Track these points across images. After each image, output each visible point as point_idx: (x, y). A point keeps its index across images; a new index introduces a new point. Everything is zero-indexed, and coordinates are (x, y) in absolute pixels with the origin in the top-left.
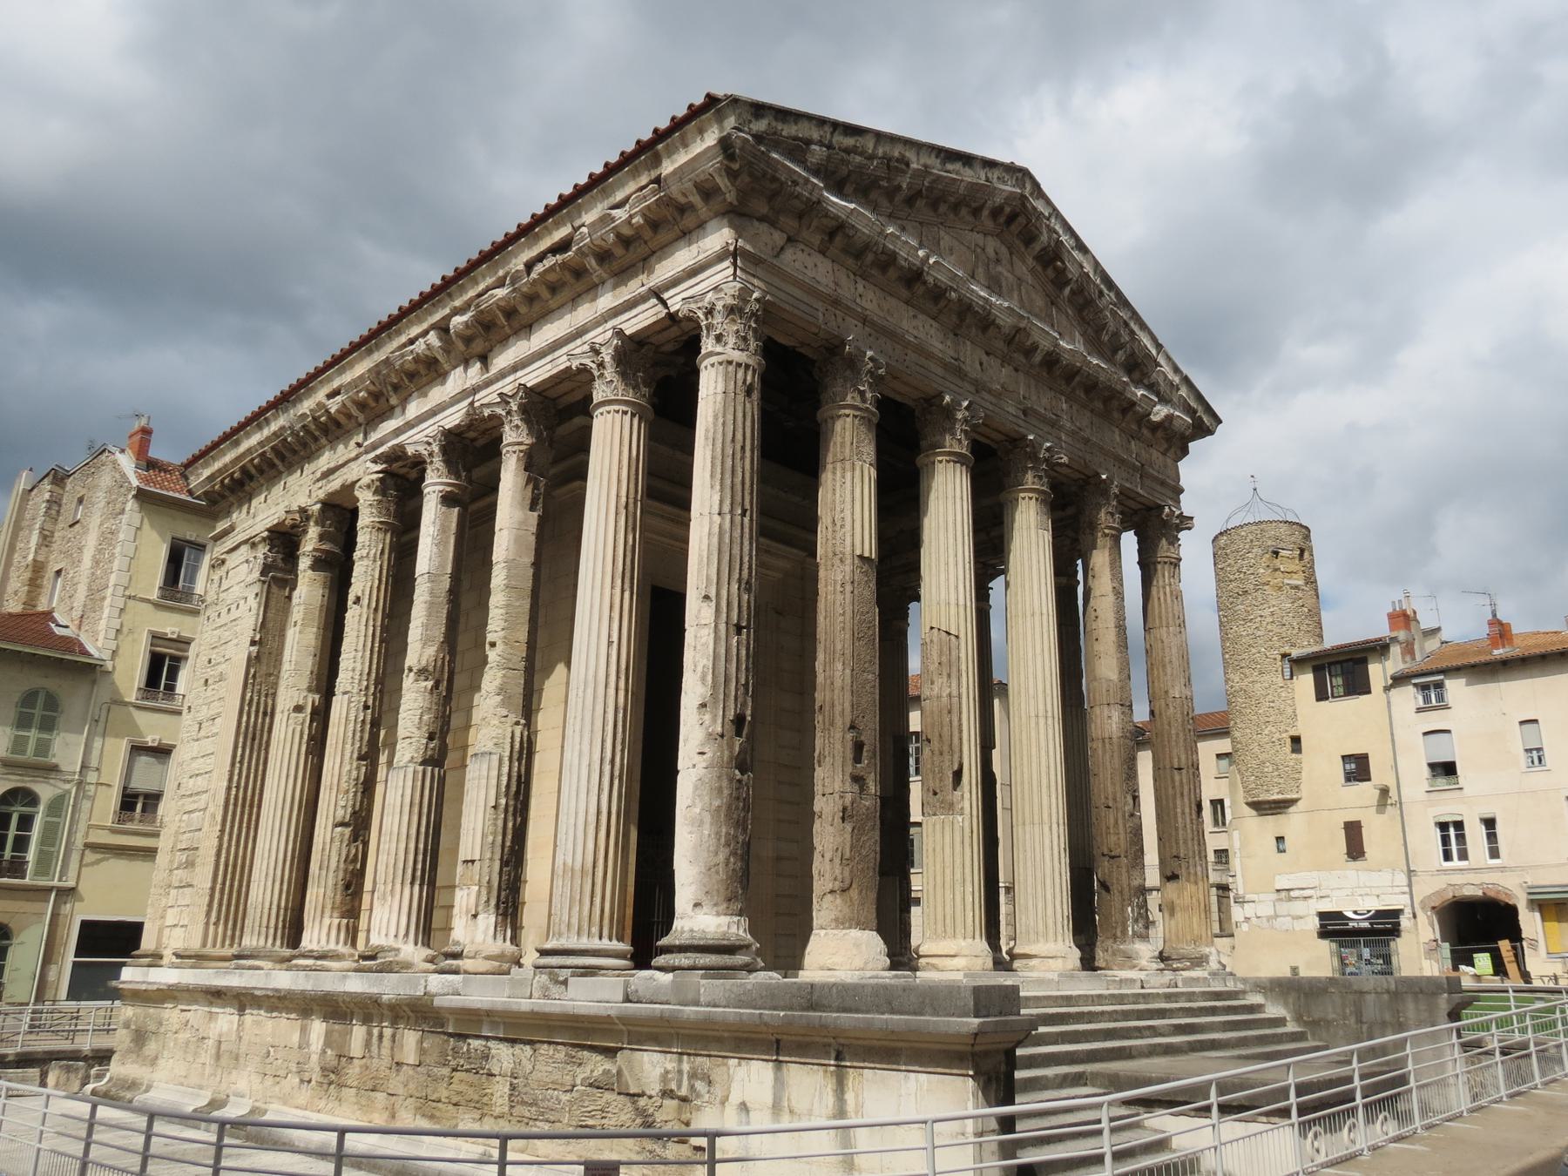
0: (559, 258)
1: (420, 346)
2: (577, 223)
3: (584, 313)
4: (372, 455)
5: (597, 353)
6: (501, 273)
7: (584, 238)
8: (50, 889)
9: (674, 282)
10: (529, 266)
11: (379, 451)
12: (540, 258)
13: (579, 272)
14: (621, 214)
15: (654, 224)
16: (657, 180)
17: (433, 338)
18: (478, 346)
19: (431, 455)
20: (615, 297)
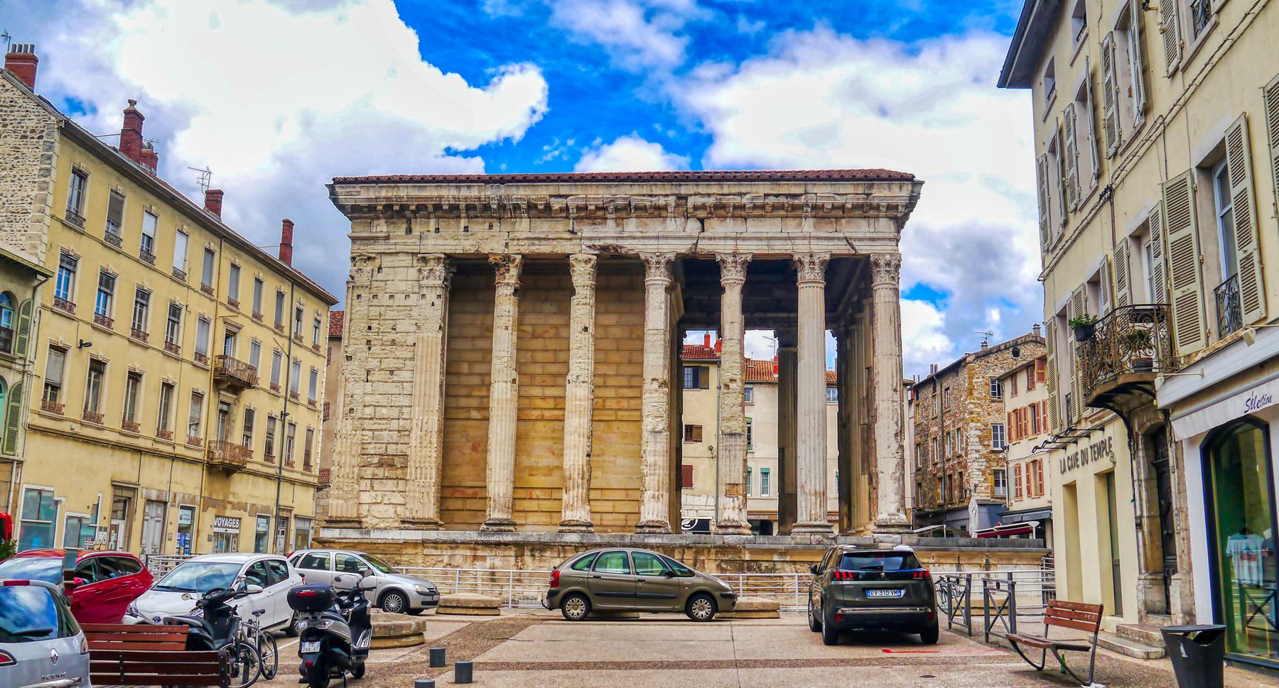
0: (791, 201)
1: (662, 202)
2: (810, 189)
3: (791, 227)
4: (590, 243)
5: (811, 256)
6: (743, 191)
7: (812, 200)
8: (12, 462)
9: (860, 239)
10: (766, 195)
11: (597, 243)
12: (777, 196)
13: (794, 208)
14: (840, 200)
15: (855, 207)
16: (868, 195)
17: (672, 200)
18: (702, 214)
19: (658, 263)
20: (815, 226)
